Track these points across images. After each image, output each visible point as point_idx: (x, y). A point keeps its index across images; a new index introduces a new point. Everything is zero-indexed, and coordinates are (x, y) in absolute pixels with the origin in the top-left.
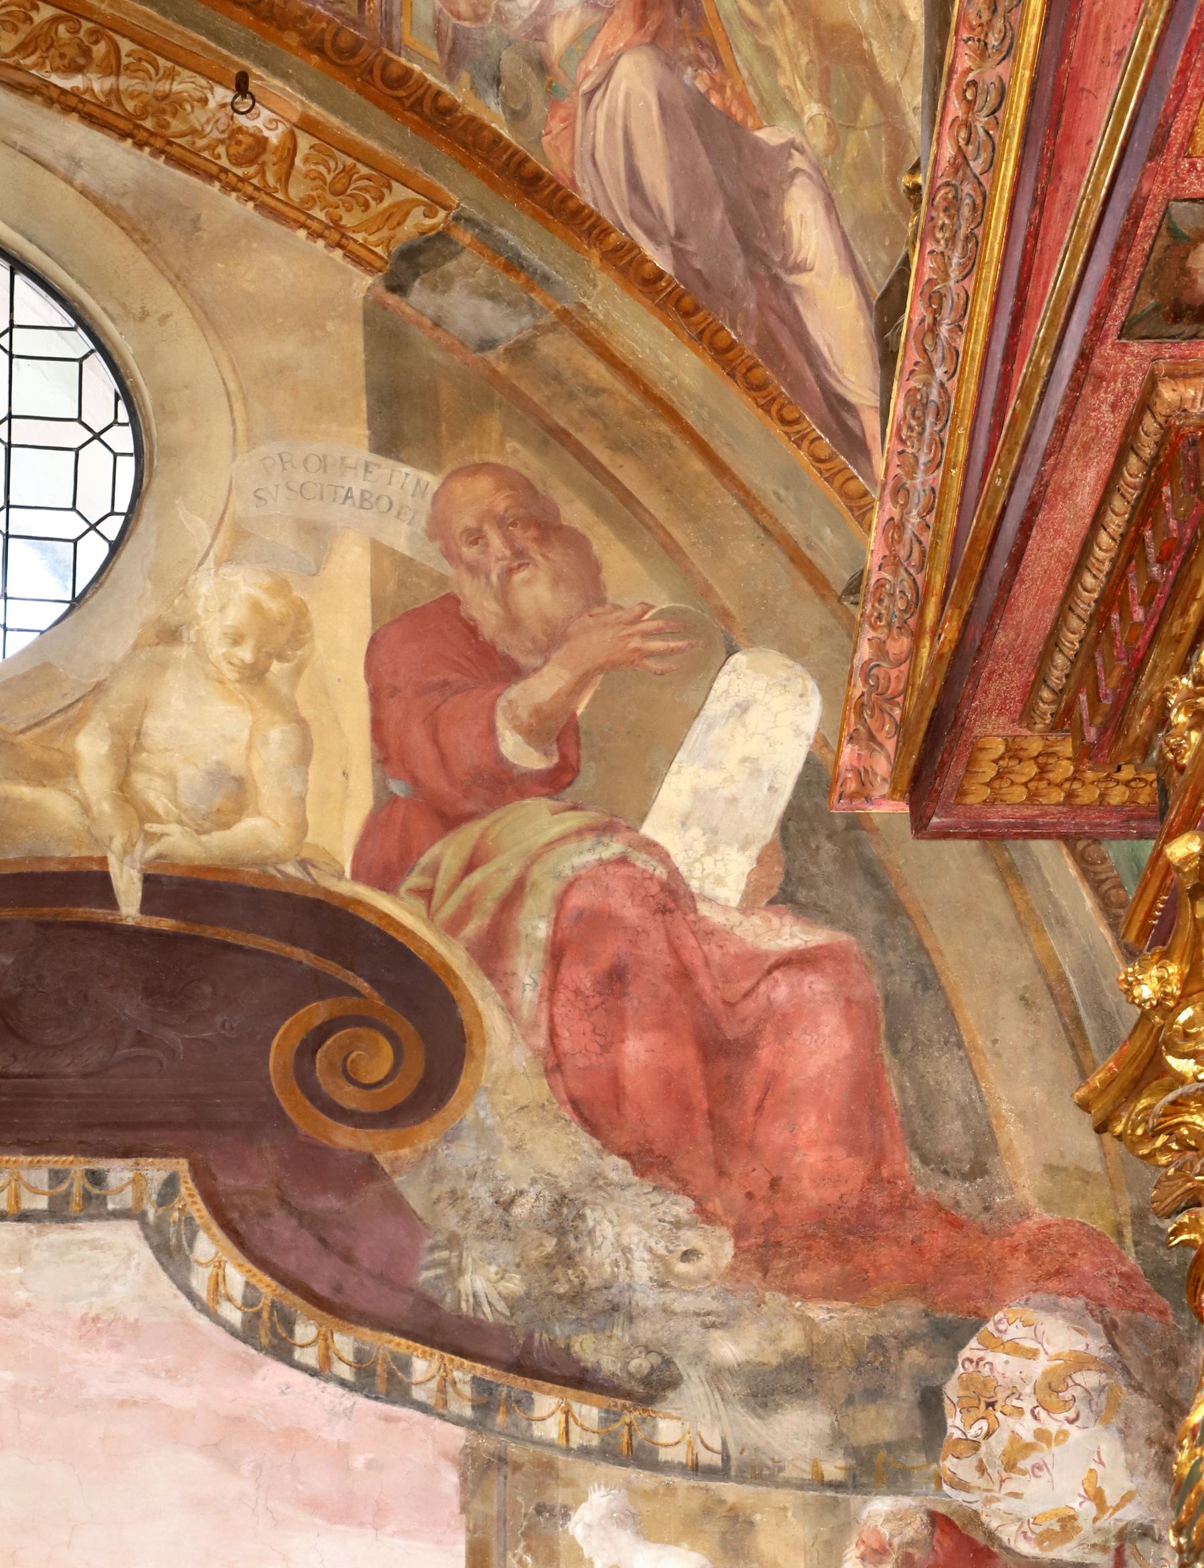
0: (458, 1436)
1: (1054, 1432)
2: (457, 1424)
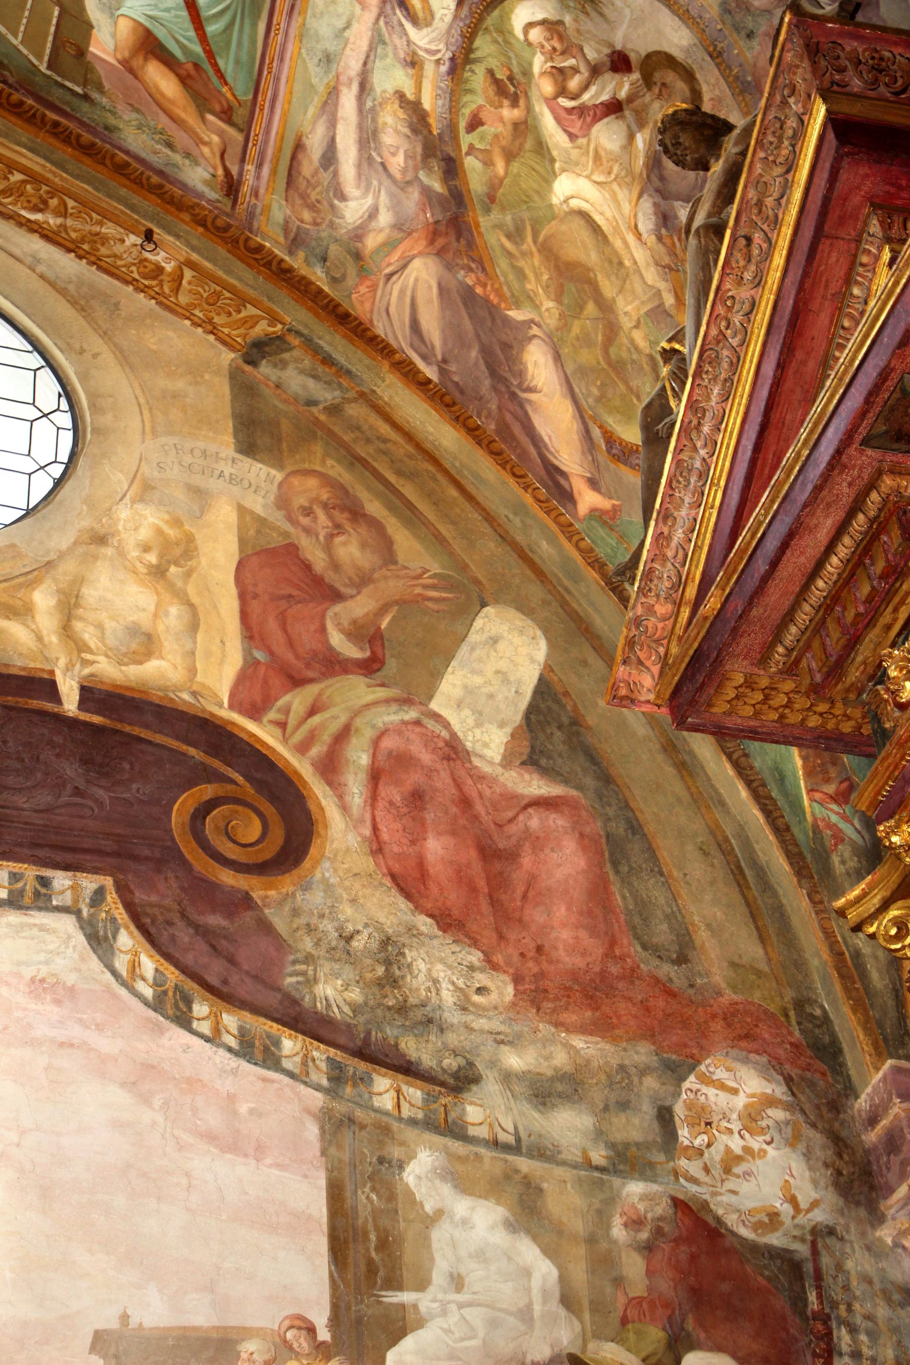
0: (317, 1099)
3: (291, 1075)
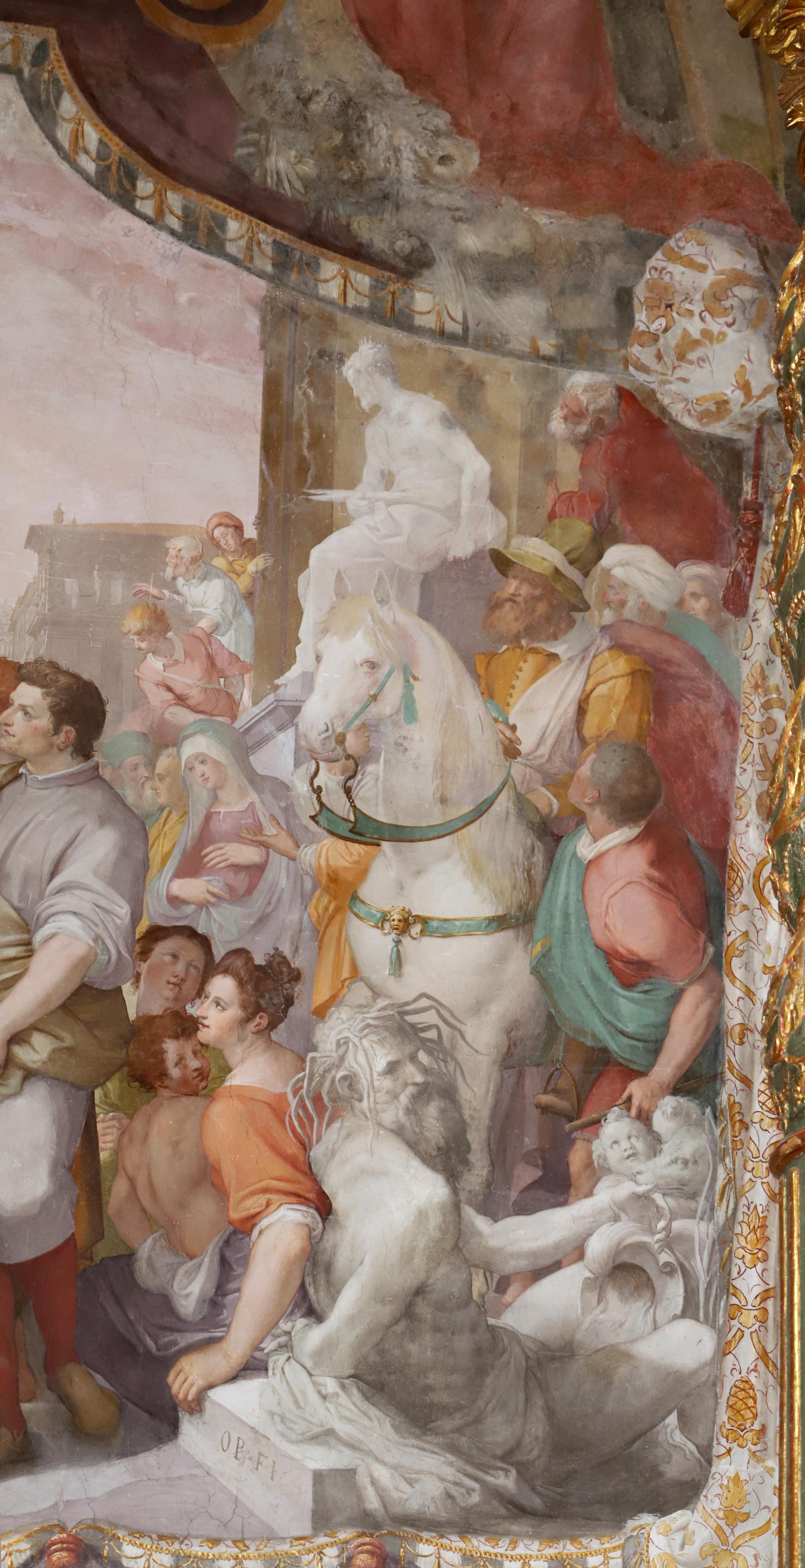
0: (260, 287)
1: (716, 334)
2: (260, 277)
3: (234, 261)
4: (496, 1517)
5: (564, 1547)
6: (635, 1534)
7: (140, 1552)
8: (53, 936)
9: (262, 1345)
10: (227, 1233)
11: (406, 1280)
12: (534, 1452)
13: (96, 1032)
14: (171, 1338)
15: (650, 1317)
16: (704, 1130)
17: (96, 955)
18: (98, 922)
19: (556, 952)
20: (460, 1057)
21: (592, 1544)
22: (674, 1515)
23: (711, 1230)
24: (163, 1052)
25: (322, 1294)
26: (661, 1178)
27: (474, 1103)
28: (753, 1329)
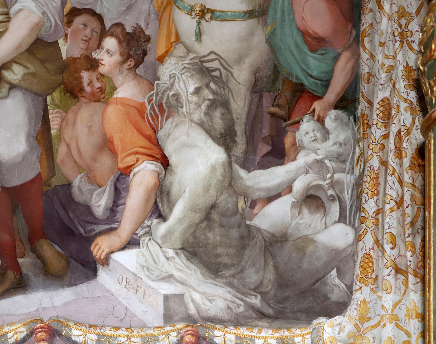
4: (251, 318)
5: (284, 333)
6: (317, 327)
7: (80, 333)
8: (20, 10)
9: (137, 232)
10: (118, 175)
11: (207, 201)
12: (269, 287)
13: (46, 65)
14: (92, 227)
15: (323, 222)
16: (349, 128)
17: (44, 22)
18: (44, 4)
19: (278, 31)
20: (231, 86)
21: (297, 331)
22: (335, 318)
23: (352, 179)
24: (81, 78)
25: (165, 207)
26: (329, 152)
27: (238, 111)
28: (372, 229)
